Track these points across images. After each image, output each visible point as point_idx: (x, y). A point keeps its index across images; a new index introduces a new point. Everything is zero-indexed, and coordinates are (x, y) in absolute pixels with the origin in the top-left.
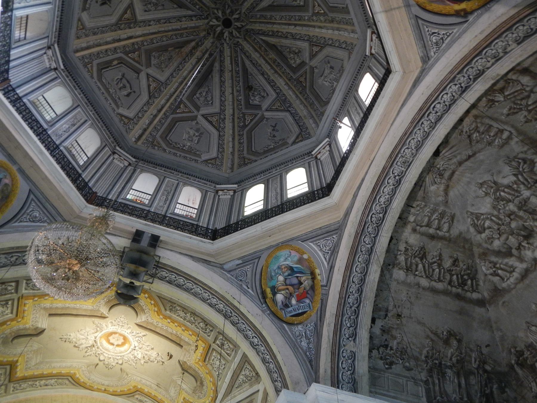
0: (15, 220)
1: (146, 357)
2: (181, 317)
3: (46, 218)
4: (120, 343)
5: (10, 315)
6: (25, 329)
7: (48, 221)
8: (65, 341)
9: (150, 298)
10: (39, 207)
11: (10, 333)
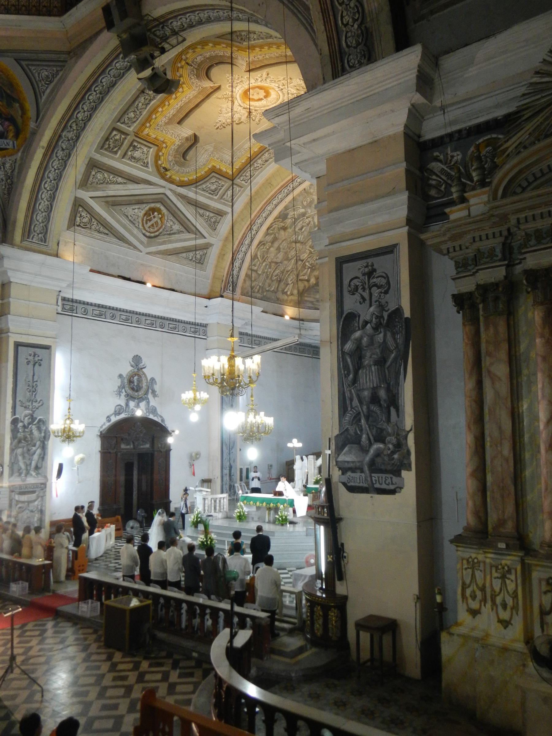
0: (39, 96)
1: (298, 88)
2: (258, 39)
3: (55, 69)
4: (264, 94)
5: (152, 150)
6: (180, 146)
7: (59, 69)
8: (224, 127)
9: (215, 44)
10: (38, 65)
11: (175, 157)
